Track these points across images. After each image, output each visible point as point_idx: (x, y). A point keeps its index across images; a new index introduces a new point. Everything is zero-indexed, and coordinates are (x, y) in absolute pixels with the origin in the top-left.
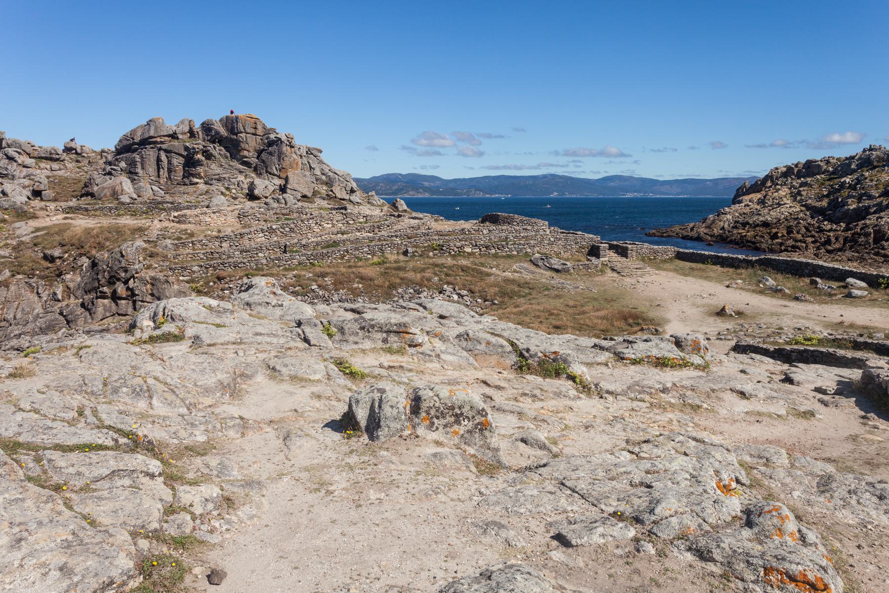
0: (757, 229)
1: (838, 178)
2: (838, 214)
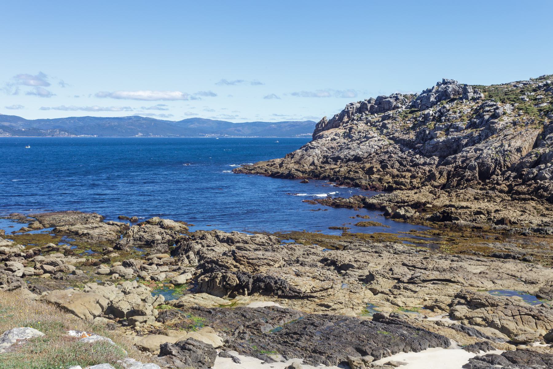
0: (350, 163)
1: (419, 111)
2: (428, 147)
